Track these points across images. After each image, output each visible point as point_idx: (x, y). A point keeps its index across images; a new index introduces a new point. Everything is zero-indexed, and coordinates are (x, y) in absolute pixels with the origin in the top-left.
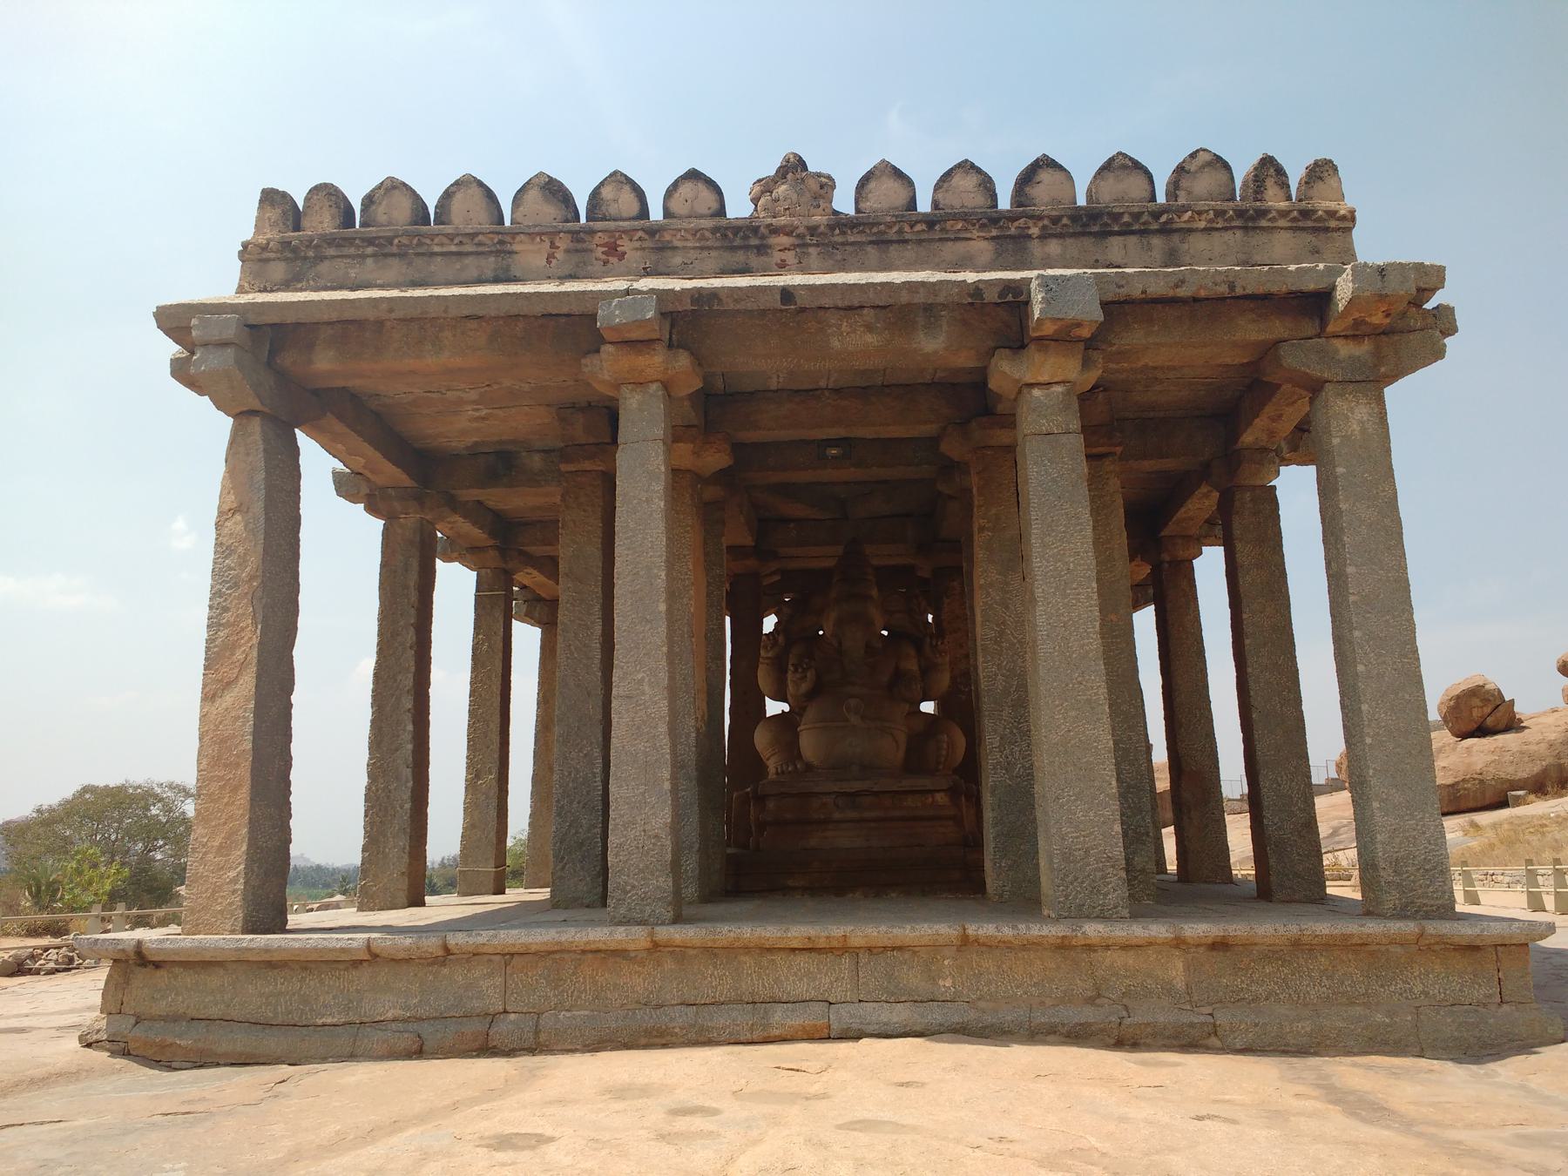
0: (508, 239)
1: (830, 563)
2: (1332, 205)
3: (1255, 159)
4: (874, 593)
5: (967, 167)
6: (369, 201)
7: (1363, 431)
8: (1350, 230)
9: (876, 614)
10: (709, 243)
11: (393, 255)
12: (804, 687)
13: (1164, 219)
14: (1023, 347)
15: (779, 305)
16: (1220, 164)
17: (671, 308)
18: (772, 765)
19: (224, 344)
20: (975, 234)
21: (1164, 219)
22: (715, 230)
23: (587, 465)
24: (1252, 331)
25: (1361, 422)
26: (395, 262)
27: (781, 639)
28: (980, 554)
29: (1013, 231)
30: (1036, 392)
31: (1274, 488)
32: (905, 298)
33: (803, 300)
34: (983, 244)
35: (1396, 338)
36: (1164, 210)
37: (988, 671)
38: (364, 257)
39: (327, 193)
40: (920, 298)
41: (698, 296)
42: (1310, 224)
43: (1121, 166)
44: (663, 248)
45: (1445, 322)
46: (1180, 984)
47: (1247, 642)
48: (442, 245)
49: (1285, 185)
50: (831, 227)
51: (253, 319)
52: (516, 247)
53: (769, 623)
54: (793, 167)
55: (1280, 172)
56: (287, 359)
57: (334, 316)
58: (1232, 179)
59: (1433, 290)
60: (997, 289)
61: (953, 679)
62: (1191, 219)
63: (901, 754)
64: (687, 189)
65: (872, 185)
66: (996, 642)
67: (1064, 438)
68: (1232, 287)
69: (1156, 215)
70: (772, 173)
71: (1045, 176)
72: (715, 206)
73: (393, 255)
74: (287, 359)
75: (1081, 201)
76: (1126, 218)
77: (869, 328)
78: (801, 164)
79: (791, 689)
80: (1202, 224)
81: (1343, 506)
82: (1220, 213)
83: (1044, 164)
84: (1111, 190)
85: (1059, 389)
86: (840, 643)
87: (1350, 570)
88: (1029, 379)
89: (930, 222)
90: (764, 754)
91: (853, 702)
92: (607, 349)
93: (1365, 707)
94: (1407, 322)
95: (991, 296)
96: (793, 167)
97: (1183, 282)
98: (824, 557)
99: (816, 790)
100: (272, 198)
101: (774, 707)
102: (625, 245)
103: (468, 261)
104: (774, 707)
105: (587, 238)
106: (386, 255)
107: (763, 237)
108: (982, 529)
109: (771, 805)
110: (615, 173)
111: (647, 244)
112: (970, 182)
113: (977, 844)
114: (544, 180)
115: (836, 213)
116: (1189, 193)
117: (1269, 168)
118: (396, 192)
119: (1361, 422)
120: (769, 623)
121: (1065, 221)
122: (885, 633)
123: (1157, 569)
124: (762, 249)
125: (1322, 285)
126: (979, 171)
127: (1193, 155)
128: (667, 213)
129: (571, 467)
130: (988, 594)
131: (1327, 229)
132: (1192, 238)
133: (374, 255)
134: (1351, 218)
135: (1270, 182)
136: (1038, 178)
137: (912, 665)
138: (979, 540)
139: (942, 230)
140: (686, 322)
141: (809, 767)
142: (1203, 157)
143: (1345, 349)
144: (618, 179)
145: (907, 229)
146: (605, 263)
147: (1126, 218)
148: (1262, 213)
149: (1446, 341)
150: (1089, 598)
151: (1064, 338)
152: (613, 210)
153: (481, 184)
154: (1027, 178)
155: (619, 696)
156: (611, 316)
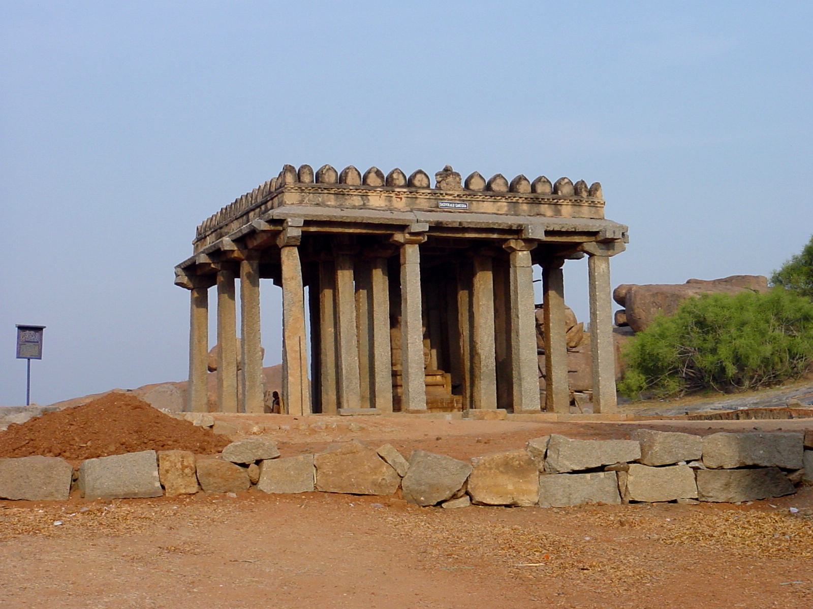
5: (499, 176)
10: (428, 197)
13: (556, 201)
15: (458, 226)
20: (504, 201)
24: (577, 239)
28: (480, 295)
30: (520, 253)
31: (562, 269)
32: (492, 226)
34: (505, 204)
50: (464, 195)
52: (369, 194)
55: (586, 187)
57: (328, 219)
60: (516, 226)
65: (473, 180)
68: (575, 228)
70: (442, 170)
72: (428, 183)
80: (565, 203)
81: (597, 294)
85: (525, 252)
87: (598, 313)
95: (514, 228)
96: (447, 171)
110: (396, 169)
111: (410, 196)
114: (376, 170)
116: (562, 192)
118: (330, 171)
119: (603, 269)
125: (597, 230)
126: (505, 179)
131: (597, 207)
135: (583, 190)
139: (495, 199)
142: (566, 180)
147: (546, 200)
152: (397, 182)
153: (356, 170)
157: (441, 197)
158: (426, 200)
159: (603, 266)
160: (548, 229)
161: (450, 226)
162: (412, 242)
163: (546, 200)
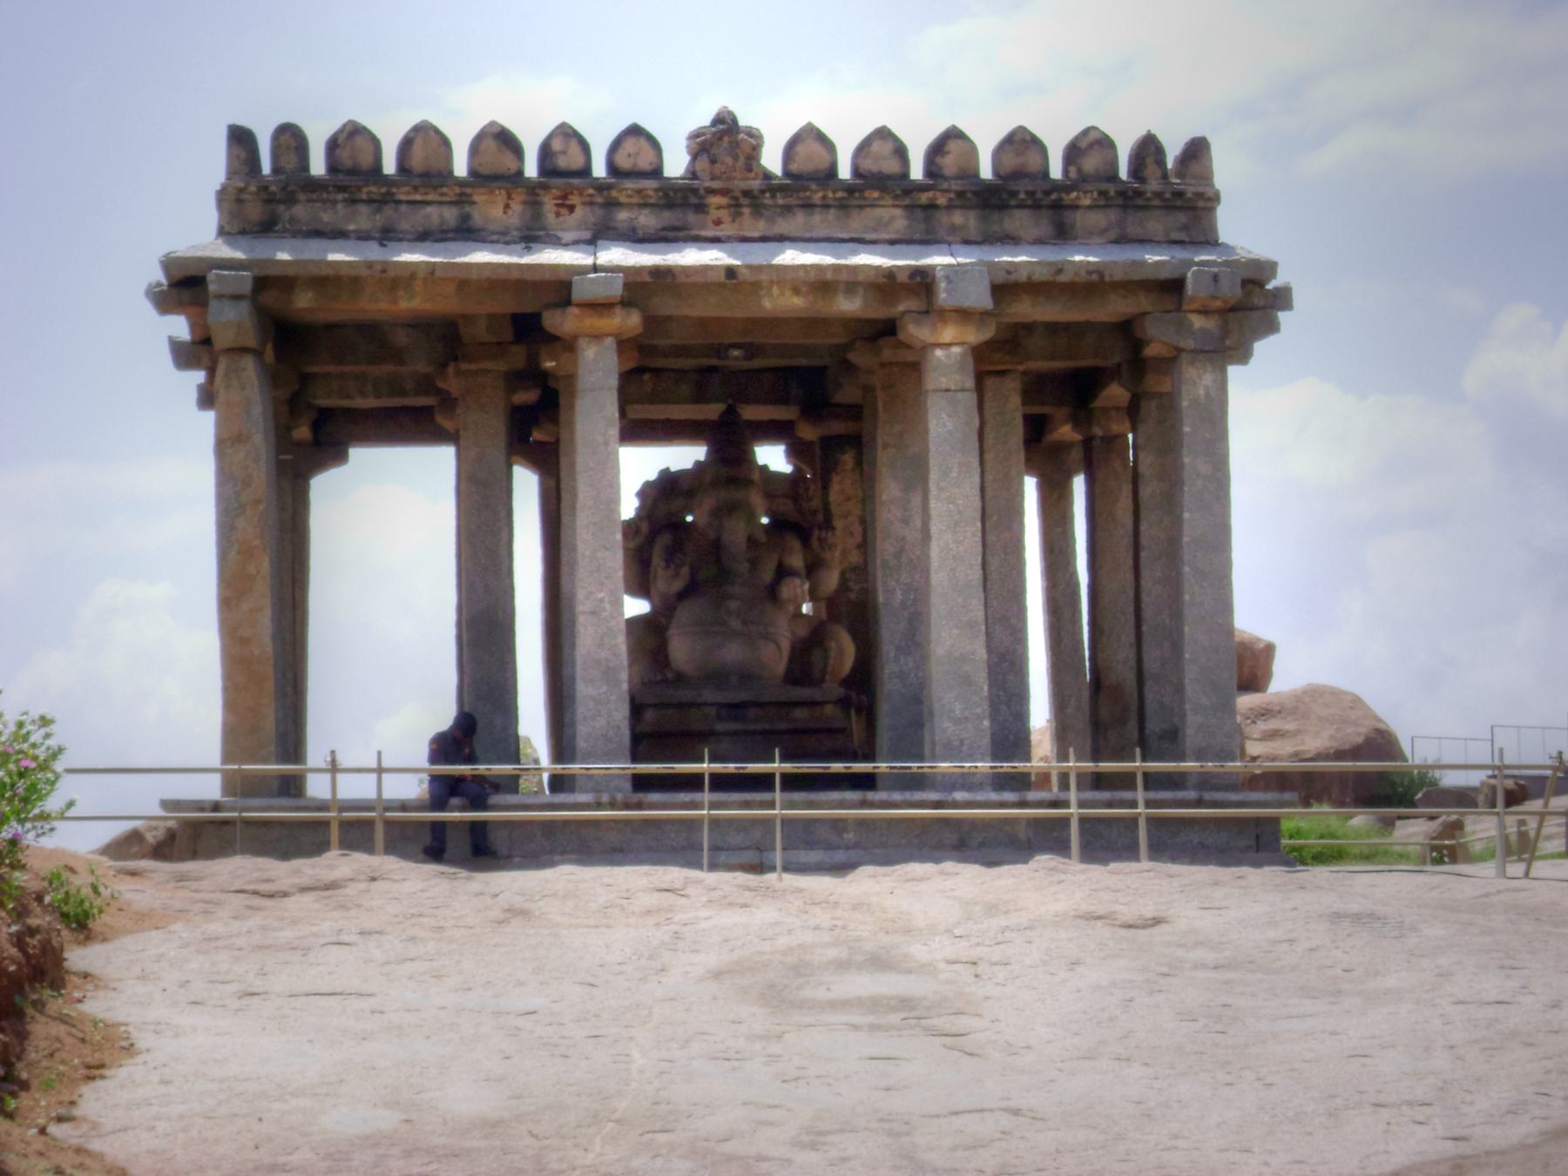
0: (468, 190)
2: (1201, 189)
3: (1137, 134)
5: (883, 134)
6: (333, 145)
7: (1208, 394)
8: (1211, 210)
9: (756, 499)
11: (362, 201)
12: (678, 585)
13: (1054, 196)
14: (927, 312)
16: (1104, 143)
17: (631, 279)
19: (237, 298)
21: (1054, 196)
22: (656, 190)
23: (490, 365)
25: (1207, 388)
26: (364, 209)
27: (645, 527)
29: (924, 198)
30: (939, 353)
33: (745, 275)
34: (898, 212)
35: (1240, 314)
36: (1057, 187)
37: (889, 593)
38: (334, 202)
39: (290, 138)
40: (844, 276)
41: (659, 273)
42: (1179, 203)
43: (1020, 142)
44: (612, 205)
45: (1282, 299)
46: (1022, 836)
47: (1143, 554)
48: (408, 193)
49: (1161, 162)
51: (257, 272)
54: (725, 125)
56: (270, 298)
58: (1115, 157)
59: (1268, 280)
61: (843, 574)
62: (1078, 198)
63: (781, 667)
64: (630, 145)
65: (800, 149)
67: (960, 395)
68: (1101, 275)
69: (1047, 193)
71: (952, 146)
73: (362, 201)
74: (270, 298)
75: (986, 172)
76: (1022, 196)
77: (796, 291)
78: (734, 120)
82: (1103, 193)
83: (953, 136)
84: (1010, 162)
85: (956, 350)
88: (931, 340)
89: (850, 189)
91: (733, 605)
92: (575, 310)
93: (1186, 629)
94: (1251, 303)
95: (903, 278)
96: (725, 125)
97: (1060, 271)
100: (241, 138)
102: (575, 200)
103: (429, 209)
105: (541, 192)
106: (354, 201)
107: (702, 198)
108: (886, 446)
109: (649, 715)
112: (888, 147)
114: (495, 130)
115: (767, 176)
116: (1079, 170)
117: (1149, 148)
119: (1207, 388)
121: (969, 195)
122: (765, 520)
123: (1087, 444)
124: (701, 208)
125: (1176, 276)
127: (1086, 132)
128: (612, 168)
129: (473, 367)
131: (1194, 208)
132: (1079, 215)
133: (345, 201)
134: (1216, 198)
135: (1150, 160)
136: (947, 148)
137: (796, 561)
140: (643, 288)
141: (680, 679)
142: (1093, 136)
143: (1198, 322)
144: (566, 133)
145: (830, 195)
146: (558, 215)
148: (1138, 194)
149: (1282, 316)
150: (974, 535)
151: (964, 315)
152: (562, 163)
153: (437, 131)
154: (938, 149)
155: (584, 613)
156: (580, 292)
157: (693, 200)
158: (646, 211)
159: (1208, 379)
160: (1013, 277)
161: (700, 279)
162: (597, 337)
163: (1022, 196)
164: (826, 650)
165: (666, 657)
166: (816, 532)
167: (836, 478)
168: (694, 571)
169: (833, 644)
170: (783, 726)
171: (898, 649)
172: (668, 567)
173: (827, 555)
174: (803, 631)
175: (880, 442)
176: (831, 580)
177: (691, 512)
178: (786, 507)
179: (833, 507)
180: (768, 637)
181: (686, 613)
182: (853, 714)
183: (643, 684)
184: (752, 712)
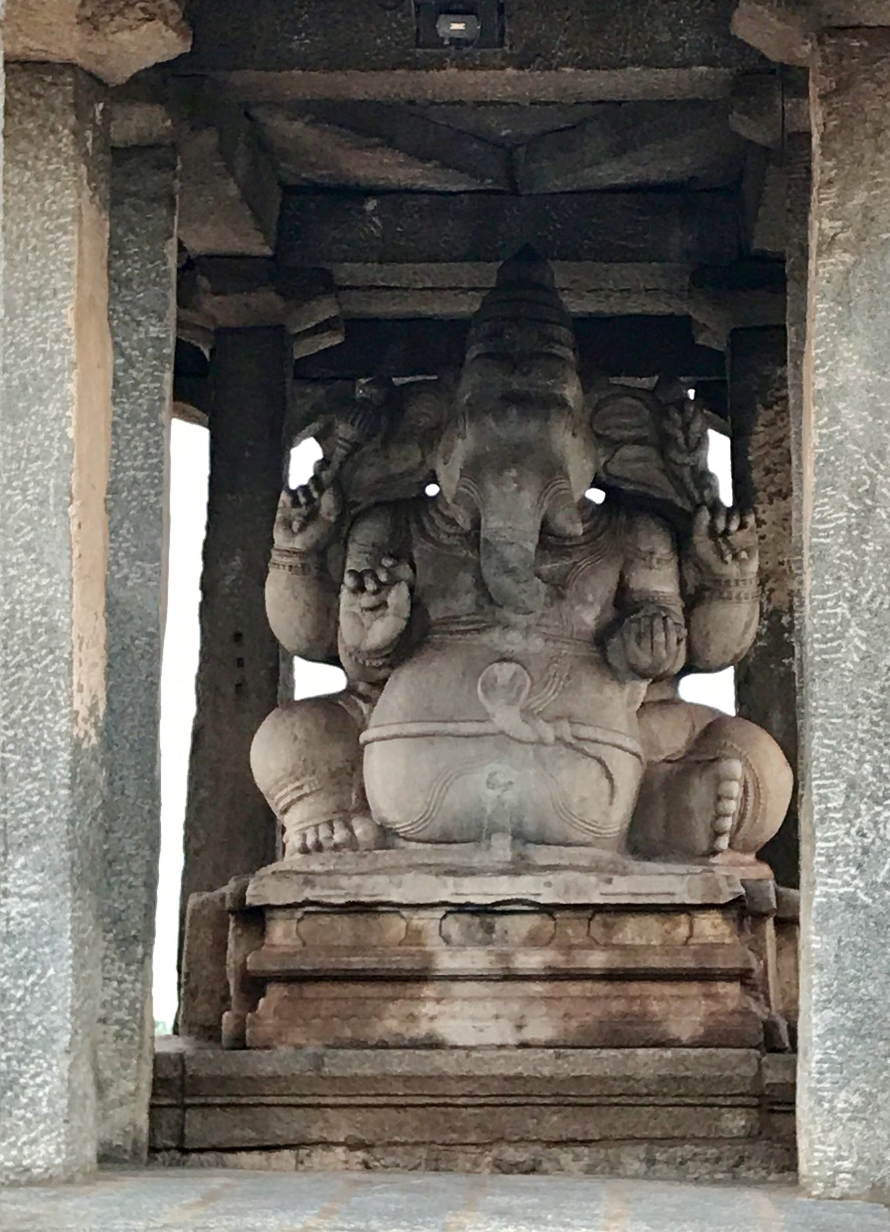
1: (466, 306)
4: (571, 392)
12: (382, 630)
18: (297, 825)
27: (327, 502)
28: (820, 309)
53: (304, 459)
66: (850, 542)
79: (348, 633)
86: (477, 525)
90: (276, 804)
98: (449, 291)
99: (395, 899)
101: (314, 679)
104: (314, 679)
108: (829, 244)
113: (777, 1040)
120: (304, 459)
130: (835, 417)
137: (660, 581)
138: (823, 271)
141: (386, 836)
164: (719, 780)
165: (363, 790)
166: (705, 517)
167: (764, 416)
168: (417, 604)
169: (736, 767)
170: (597, 960)
171: (852, 785)
172: (360, 589)
173: (731, 570)
174: (674, 738)
175: (813, 244)
176: (738, 621)
177: (433, 479)
178: (636, 463)
179: (756, 475)
180: (576, 747)
181: (400, 692)
182: (769, 927)
183: (305, 850)
184: (520, 926)
